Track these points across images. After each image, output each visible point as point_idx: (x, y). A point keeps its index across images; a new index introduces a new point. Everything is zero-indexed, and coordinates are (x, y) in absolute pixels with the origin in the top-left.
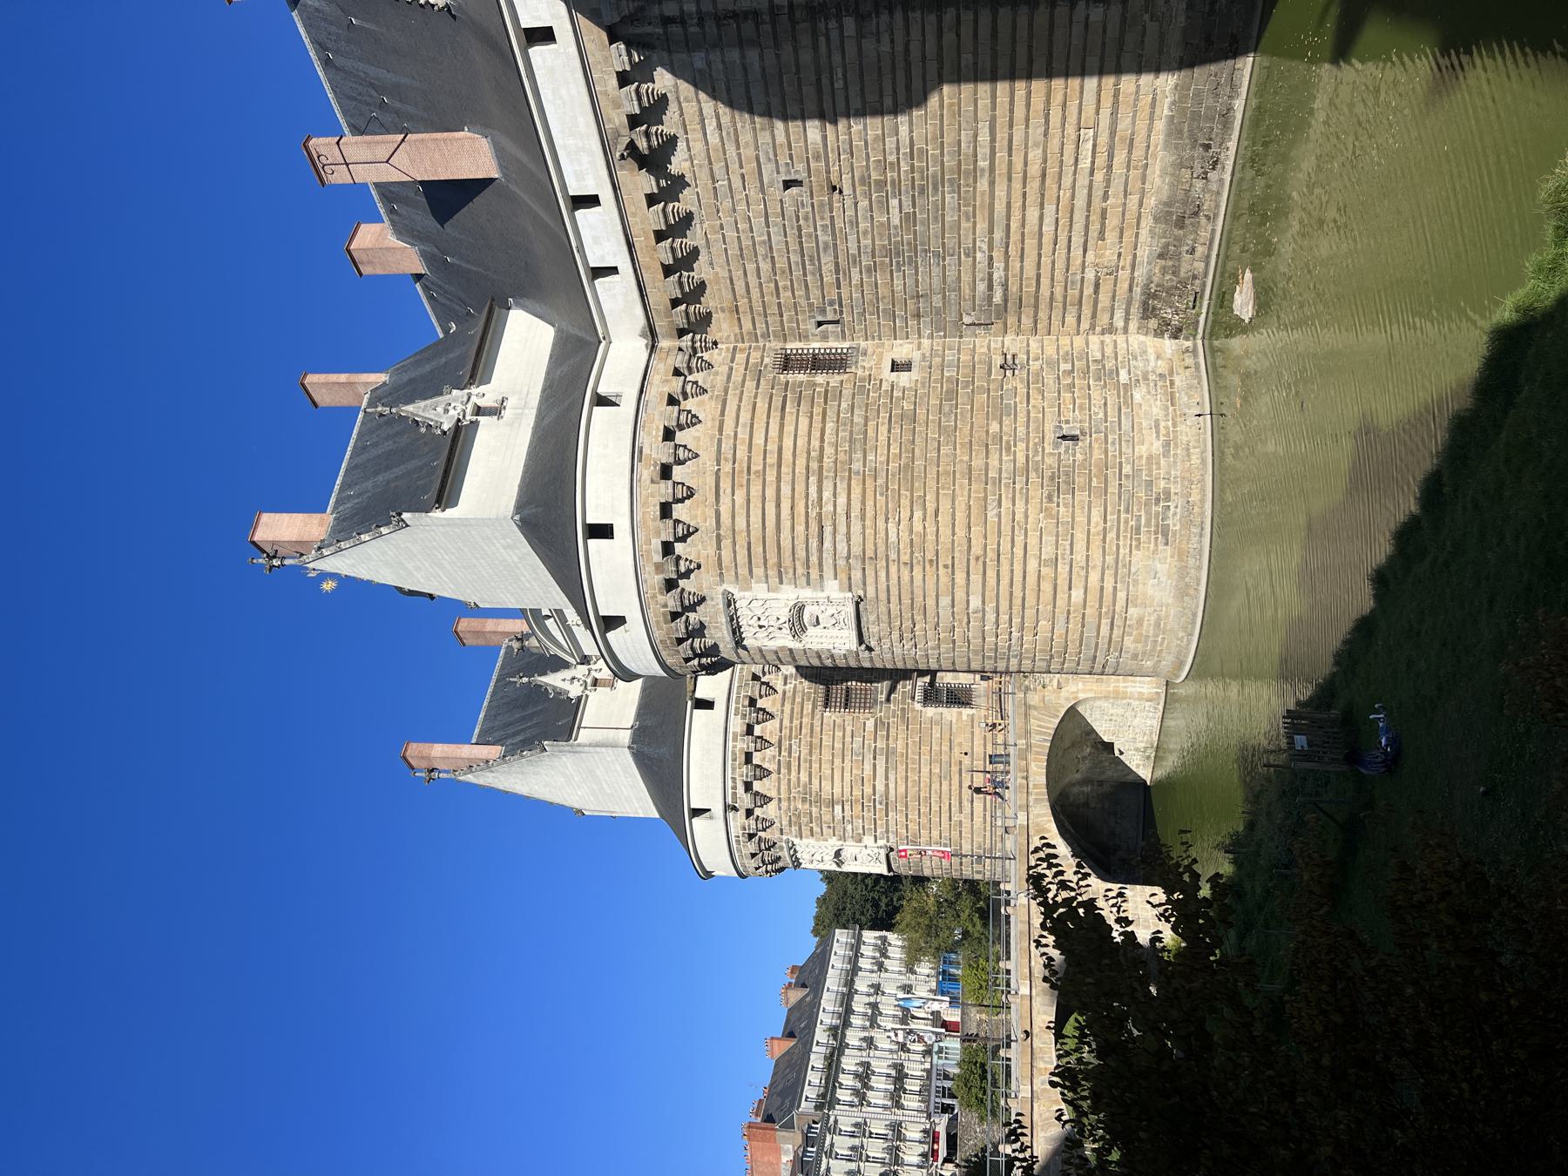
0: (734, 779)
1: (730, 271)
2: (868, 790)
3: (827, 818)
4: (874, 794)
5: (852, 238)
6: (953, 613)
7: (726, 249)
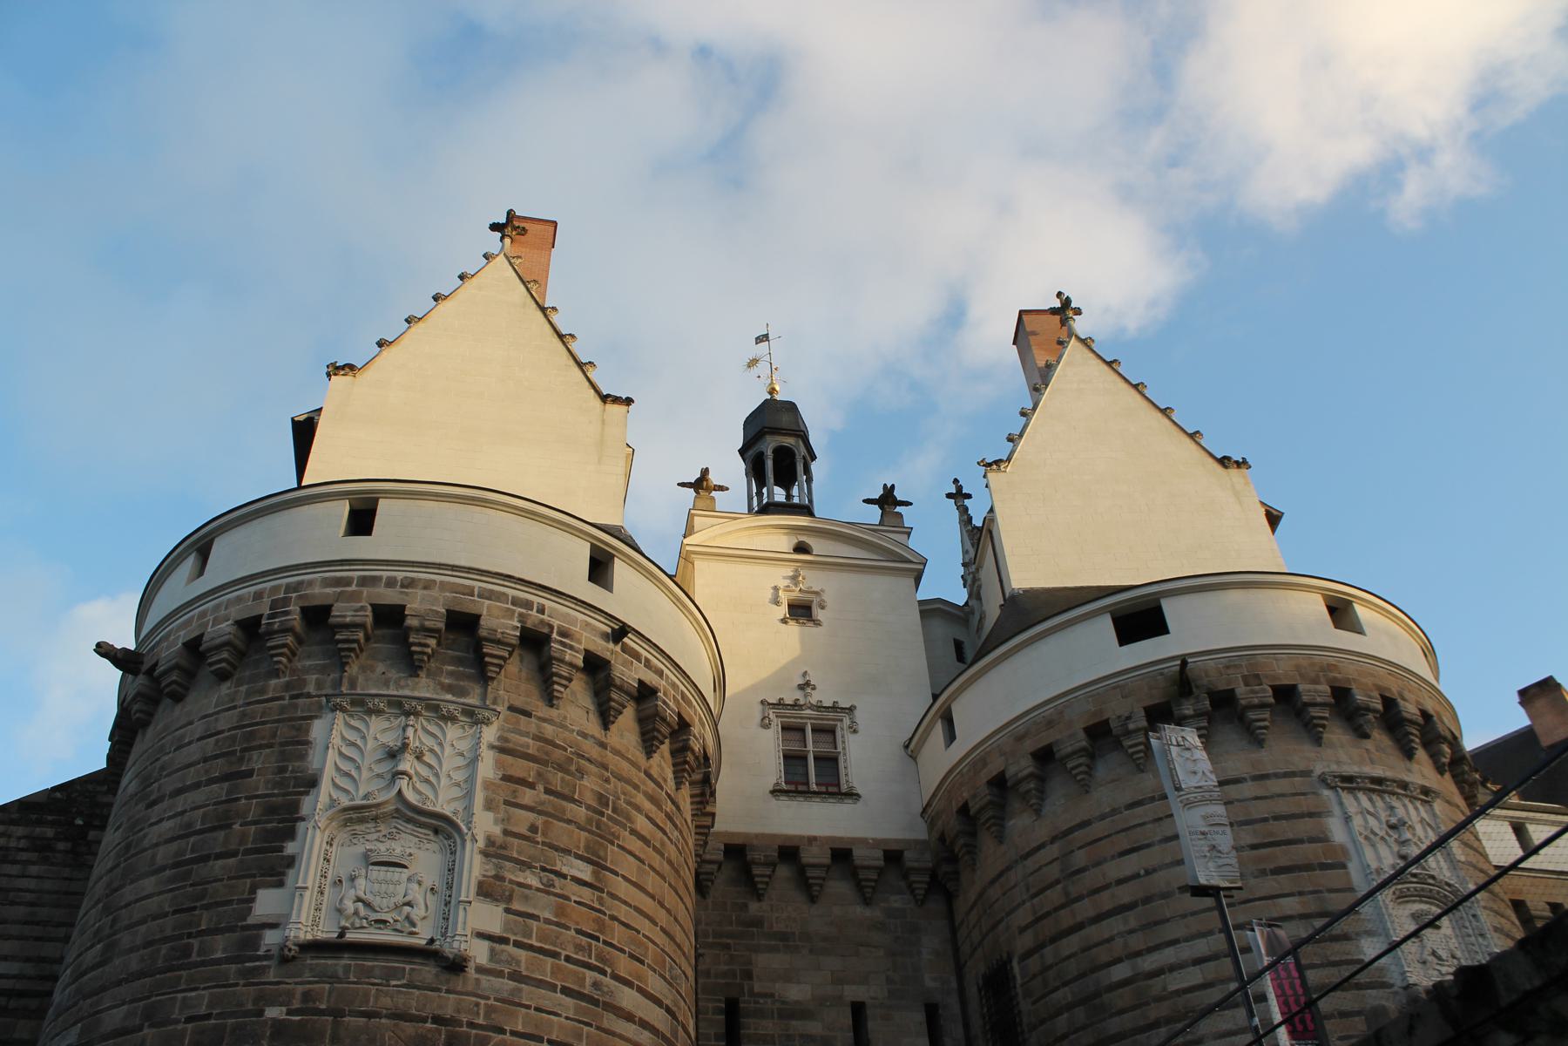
3: (562, 833)
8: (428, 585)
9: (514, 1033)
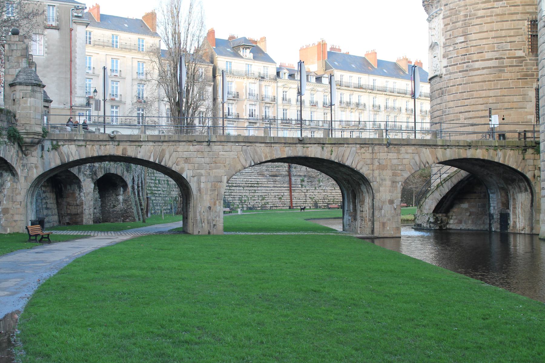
2: (475, 57)
4: (473, 62)
9: (451, 86)
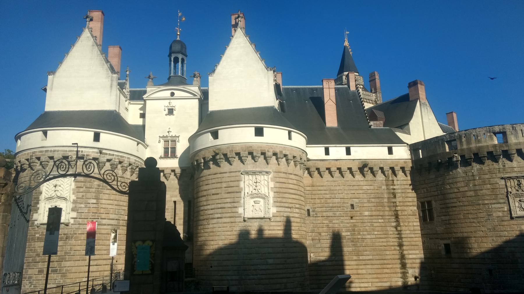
0: (113, 155)
1: (326, 186)
2: (103, 216)
3: (89, 195)
5: (337, 221)
6: (266, 253)
7: (333, 186)
8: (58, 151)
9: (78, 234)
